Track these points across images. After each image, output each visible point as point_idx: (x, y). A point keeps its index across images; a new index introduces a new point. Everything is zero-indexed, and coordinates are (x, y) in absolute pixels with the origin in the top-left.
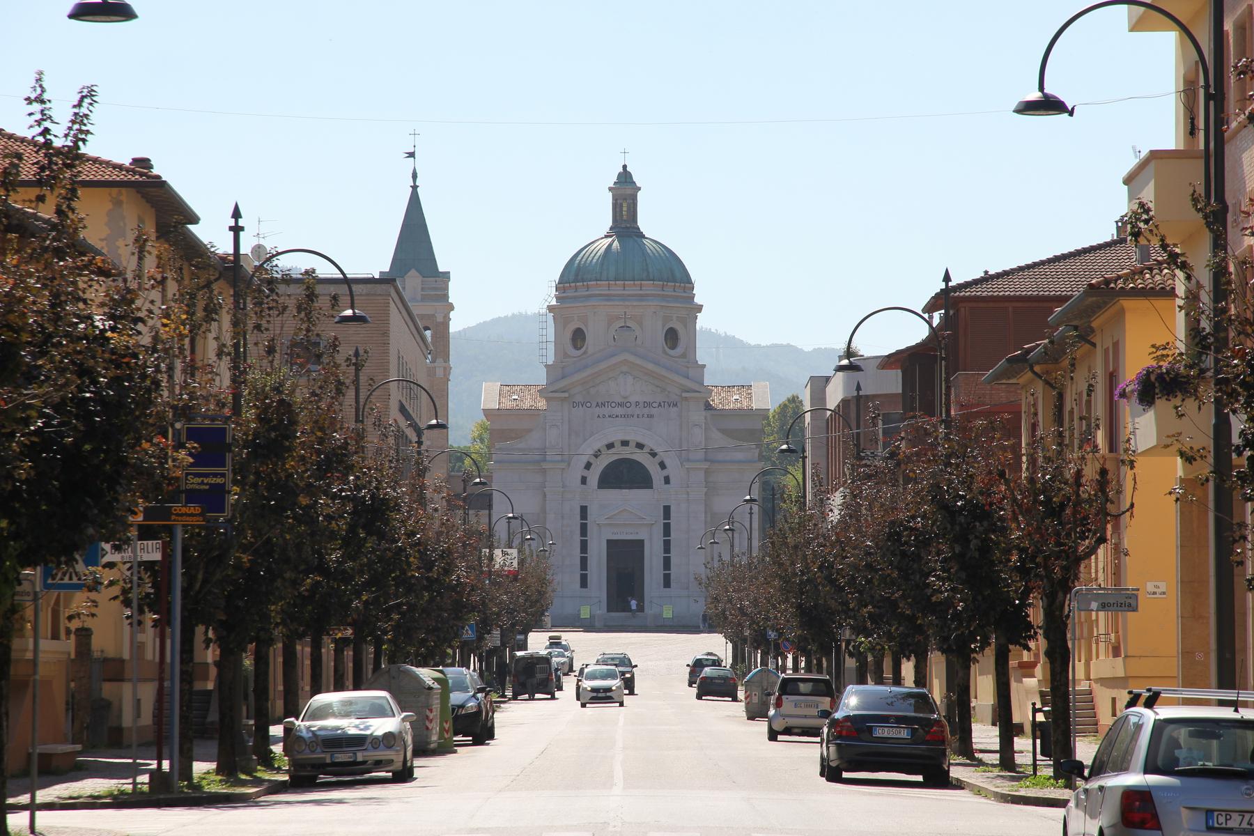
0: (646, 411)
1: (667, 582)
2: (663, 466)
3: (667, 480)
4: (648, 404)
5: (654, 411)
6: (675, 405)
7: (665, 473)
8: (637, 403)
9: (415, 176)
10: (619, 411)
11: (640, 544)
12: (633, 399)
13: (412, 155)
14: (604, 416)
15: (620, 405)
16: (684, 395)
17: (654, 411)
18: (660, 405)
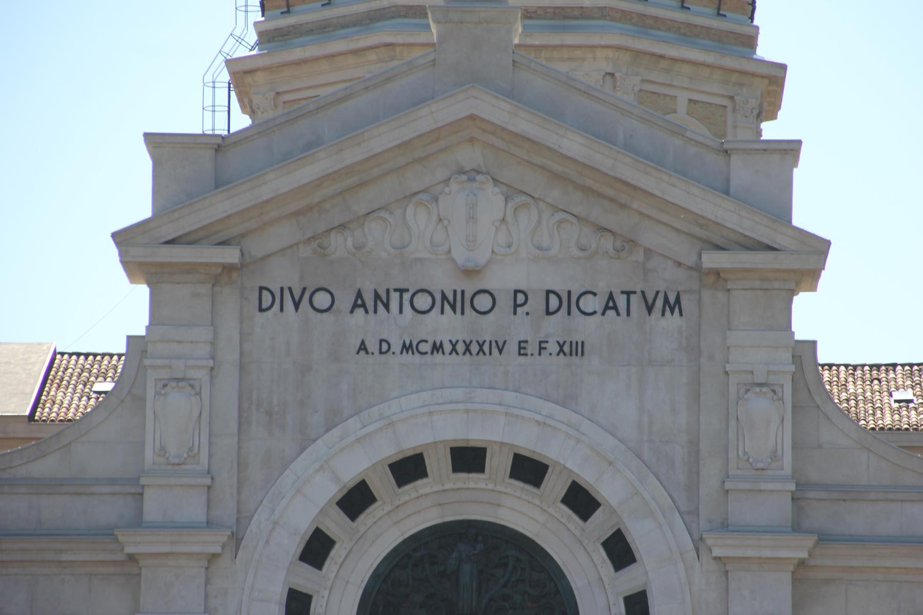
0: (554, 328)
4: (560, 302)
8: (519, 299)
12: (504, 279)
14: (384, 347)
15: (452, 302)
18: (610, 304)
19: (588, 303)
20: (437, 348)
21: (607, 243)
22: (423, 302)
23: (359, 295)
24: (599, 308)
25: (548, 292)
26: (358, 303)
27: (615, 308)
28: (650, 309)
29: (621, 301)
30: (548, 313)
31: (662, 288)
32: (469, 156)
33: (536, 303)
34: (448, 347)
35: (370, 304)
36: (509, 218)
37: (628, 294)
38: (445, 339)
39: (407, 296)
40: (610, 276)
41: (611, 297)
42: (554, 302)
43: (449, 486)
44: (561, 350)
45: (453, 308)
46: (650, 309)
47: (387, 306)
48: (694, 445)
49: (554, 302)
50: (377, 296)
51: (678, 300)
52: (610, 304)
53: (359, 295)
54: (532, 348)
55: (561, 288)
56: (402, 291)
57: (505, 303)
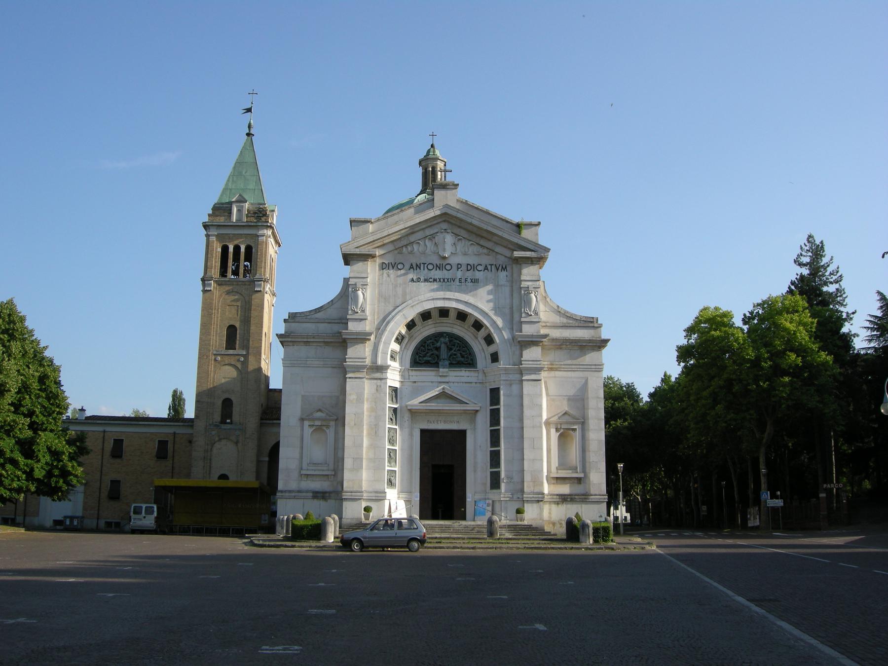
0: (469, 274)
1: (495, 482)
2: (489, 340)
3: (495, 358)
4: (471, 267)
5: (479, 275)
6: (504, 269)
7: (492, 349)
8: (459, 266)
9: (250, 127)
10: (437, 274)
11: (463, 433)
12: (454, 261)
13: (249, 110)
14: (419, 280)
15: (439, 267)
16: (517, 254)
17: (479, 275)
18: (486, 268)
19: (479, 268)
20: (435, 280)
21: (485, 251)
22: (430, 267)
26: (411, 267)
29: (489, 267)
32: (444, 226)
33: (464, 268)
38: (437, 277)
40: (486, 260)
48: (511, 308)
52: (486, 268)
54: (463, 281)
55: (471, 263)
57: (455, 267)
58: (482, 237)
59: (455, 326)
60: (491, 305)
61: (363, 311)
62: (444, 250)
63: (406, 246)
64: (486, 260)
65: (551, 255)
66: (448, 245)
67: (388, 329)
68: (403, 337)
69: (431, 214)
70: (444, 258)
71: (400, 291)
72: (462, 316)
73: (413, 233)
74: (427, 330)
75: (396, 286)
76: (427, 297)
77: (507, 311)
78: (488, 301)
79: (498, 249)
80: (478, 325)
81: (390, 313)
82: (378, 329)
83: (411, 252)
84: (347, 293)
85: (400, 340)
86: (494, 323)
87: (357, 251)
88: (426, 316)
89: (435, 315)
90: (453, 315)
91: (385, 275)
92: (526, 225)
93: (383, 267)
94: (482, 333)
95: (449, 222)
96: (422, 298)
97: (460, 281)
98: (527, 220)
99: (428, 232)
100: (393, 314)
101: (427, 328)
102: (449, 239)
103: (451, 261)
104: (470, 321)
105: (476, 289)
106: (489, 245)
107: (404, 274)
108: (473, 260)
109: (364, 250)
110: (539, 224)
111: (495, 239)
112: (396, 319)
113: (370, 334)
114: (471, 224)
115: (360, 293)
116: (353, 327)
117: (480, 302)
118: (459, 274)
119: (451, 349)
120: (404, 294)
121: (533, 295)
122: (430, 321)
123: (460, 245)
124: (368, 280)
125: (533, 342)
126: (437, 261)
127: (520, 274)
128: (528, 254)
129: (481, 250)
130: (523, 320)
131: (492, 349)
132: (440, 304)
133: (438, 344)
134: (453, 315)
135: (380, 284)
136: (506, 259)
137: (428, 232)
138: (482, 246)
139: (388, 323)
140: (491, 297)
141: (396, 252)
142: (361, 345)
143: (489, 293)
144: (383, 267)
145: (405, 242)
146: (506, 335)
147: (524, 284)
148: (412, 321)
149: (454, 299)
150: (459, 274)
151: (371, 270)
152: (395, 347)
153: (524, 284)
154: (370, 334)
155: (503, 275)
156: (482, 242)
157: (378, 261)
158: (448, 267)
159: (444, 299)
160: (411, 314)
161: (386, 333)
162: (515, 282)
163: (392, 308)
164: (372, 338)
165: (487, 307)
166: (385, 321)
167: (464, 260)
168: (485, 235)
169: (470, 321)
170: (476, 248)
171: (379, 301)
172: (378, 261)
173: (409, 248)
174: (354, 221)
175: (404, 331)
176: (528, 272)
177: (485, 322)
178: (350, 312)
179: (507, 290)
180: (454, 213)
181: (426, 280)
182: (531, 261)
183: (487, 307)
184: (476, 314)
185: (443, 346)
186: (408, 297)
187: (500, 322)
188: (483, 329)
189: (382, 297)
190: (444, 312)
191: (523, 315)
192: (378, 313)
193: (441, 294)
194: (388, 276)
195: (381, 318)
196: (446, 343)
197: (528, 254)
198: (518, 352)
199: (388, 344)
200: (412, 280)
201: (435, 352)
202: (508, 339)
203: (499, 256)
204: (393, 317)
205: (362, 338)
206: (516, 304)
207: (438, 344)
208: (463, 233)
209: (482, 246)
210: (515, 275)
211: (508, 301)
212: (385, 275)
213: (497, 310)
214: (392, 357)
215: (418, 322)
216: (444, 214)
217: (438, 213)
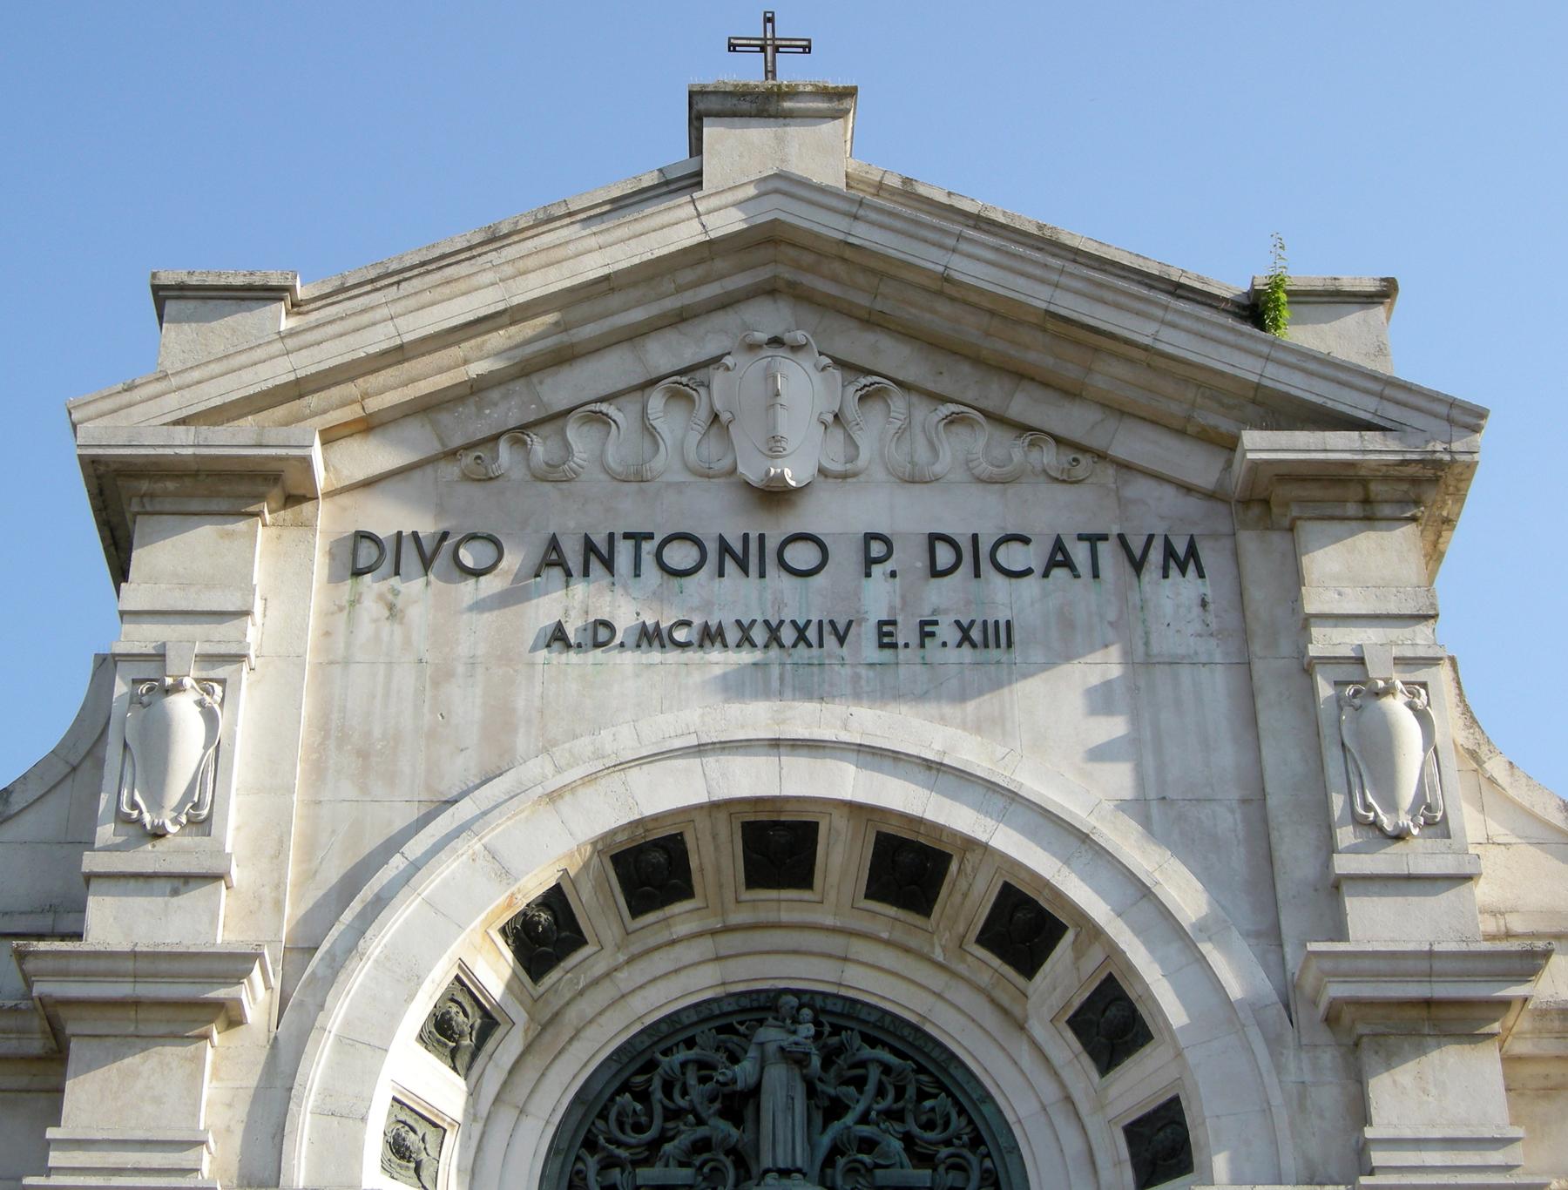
0: (948, 598)
2: (1112, 1024)
7: (1137, 1084)
8: (875, 550)
10: (732, 597)
12: (838, 516)
14: (600, 634)
15: (736, 556)
16: (1262, 445)
17: (1003, 599)
18: (1059, 558)
19: (1013, 556)
20: (711, 636)
21: (1049, 456)
22: (680, 556)
23: (554, 544)
24: (1038, 565)
25: (934, 538)
26: (552, 558)
27: (1068, 563)
28: (1138, 565)
29: (1080, 553)
30: (936, 573)
31: (1160, 529)
32: (768, 318)
33: (909, 557)
34: (732, 635)
35: (574, 562)
36: (852, 409)
37: (1093, 539)
38: (724, 616)
39: (648, 548)
40: (1052, 512)
41: (1059, 546)
42: (944, 556)
43: (736, 918)
44: (966, 638)
45: (743, 566)
46: (1138, 565)
47: (609, 564)
48: (1256, 801)
49: (944, 556)
50: (590, 547)
51: (1192, 551)
52: (1059, 558)
53: (554, 544)
54: (906, 633)
55: (959, 529)
56: (638, 538)
57: (845, 558)
58: (1021, 375)
59: (859, 948)
60: (1119, 778)
61: (200, 824)
62: (773, 446)
63: (519, 434)
64: (1052, 512)
65: (1489, 449)
66: (796, 411)
67: (378, 942)
68: (489, 1022)
69: (676, 229)
70: (774, 496)
71: (467, 704)
72: (909, 867)
73: (563, 358)
74: (656, 977)
75: (443, 675)
76: (672, 734)
77: (1227, 820)
78: (1099, 754)
79: (1133, 443)
80: (1025, 927)
81: (393, 845)
82: (301, 948)
83: (554, 475)
84: (111, 730)
85: (459, 1030)
86: (1139, 896)
87: (185, 443)
88: (649, 868)
89: (716, 859)
90: (842, 860)
91: (371, 607)
92: (1302, 297)
93: (361, 557)
94: (1063, 977)
95: (800, 296)
96: (622, 741)
97: (886, 635)
98: (1304, 272)
99: (664, 354)
100: (416, 847)
101: (661, 962)
102: (804, 388)
103: (817, 516)
104: (968, 899)
105: (997, 685)
106: (1075, 420)
107: (510, 598)
108: (970, 514)
109: (235, 440)
110: (1385, 292)
111: (1108, 376)
112: (433, 882)
113: (236, 965)
114: (945, 287)
115: (184, 709)
116: (111, 923)
117: (1041, 758)
118: (877, 597)
119: (835, 1110)
120: (499, 722)
121: (1397, 706)
122: (681, 917)
123: (874, 431)
124: (254, 633)
125: (1436, 1008)
126: (721, 517)
127: (1297, 579)
128: (1338, 446)
129: (1017, 452)
130: (1344, 864)
131: (1137, 1084)
132: (750, 779)
133: (745, 1071)
134: (842, 860)
135: (335, 663)
136: (1192, 505)
137: (664, 354)
138: (1023, 428)
139: (380, 903)
140: (1115, 727)
141: (451, 471)
142: (171, 1053)
143: (1101, 700)
144: (361, 557)
145: (508, 411)
146: (1235, 973)
147: (1323, 642)
148: (555, 899)
149: (856, 749)
150: (877, 597)
151: (274, 575)
152: (442, 1088)
153: (1325, 642)
154: (236, 965)
155: (1174, 596)
156: (1022, 406)
157: (328, 521)
158: (801, 556)
159: (776, 744)
160: (546, 847)
161: (359, 978)
162: (1267, 645)
163: (413, 813)
164: (256, 998)
165: (1092, 794)
166: (354, 894)
167: (906, 515)
168: (1037, 355)
169: (968, 899)
170: (981, 445)
171: (318, 771)
172: (328, 521)
173: (540, 448)
174: (182, 291)
175: (495, 971)
176: (1347, 572)
177: (1080, 891)
178: (106, 832)
179: (1217, 687)
180: (831, 226)
181: (650, 637)
182: (1359, 498)
183: (1092, 794)
184: (1008, 841)
185: (778, 1080)
186: (522, 742)
187: (1185, 894)
188: (1063, 950)
189: (347, 747)
190: (778, 845)
191: (1346, 835)
192: (310, 847)
193: (757, 717)
194: (393, 612)
195: (332, 873)
196: (797, 1060)
197: (1338, 446)
198: (1329, 1096)
199: (366, 1046)
200: (558, 637)
201: (722, 1129)
202: (1255, 1007)
203: (1140, 488)
204: (415, 867)
205: (179, 1002)
206: (1291, 771)
207: (745, 1071)
208: (894, 357)
209: (1023, 428)
210: (1258, 595)
211: (1227, 757)
212: (371, 607)
213: (1155, 809)
214: (398, 1149)
215: (598, 909)
216: (764, 240)
217: (728, 222)
